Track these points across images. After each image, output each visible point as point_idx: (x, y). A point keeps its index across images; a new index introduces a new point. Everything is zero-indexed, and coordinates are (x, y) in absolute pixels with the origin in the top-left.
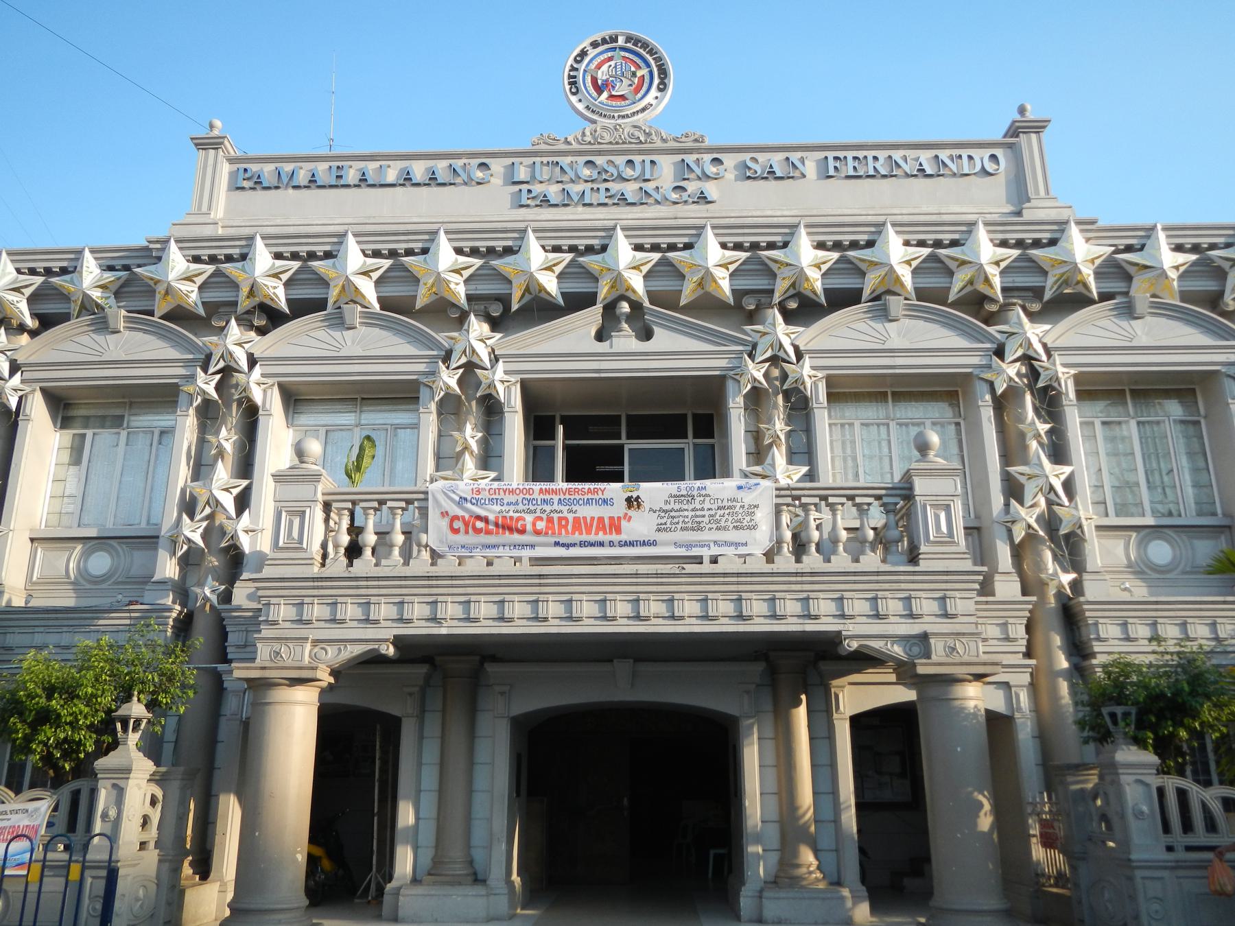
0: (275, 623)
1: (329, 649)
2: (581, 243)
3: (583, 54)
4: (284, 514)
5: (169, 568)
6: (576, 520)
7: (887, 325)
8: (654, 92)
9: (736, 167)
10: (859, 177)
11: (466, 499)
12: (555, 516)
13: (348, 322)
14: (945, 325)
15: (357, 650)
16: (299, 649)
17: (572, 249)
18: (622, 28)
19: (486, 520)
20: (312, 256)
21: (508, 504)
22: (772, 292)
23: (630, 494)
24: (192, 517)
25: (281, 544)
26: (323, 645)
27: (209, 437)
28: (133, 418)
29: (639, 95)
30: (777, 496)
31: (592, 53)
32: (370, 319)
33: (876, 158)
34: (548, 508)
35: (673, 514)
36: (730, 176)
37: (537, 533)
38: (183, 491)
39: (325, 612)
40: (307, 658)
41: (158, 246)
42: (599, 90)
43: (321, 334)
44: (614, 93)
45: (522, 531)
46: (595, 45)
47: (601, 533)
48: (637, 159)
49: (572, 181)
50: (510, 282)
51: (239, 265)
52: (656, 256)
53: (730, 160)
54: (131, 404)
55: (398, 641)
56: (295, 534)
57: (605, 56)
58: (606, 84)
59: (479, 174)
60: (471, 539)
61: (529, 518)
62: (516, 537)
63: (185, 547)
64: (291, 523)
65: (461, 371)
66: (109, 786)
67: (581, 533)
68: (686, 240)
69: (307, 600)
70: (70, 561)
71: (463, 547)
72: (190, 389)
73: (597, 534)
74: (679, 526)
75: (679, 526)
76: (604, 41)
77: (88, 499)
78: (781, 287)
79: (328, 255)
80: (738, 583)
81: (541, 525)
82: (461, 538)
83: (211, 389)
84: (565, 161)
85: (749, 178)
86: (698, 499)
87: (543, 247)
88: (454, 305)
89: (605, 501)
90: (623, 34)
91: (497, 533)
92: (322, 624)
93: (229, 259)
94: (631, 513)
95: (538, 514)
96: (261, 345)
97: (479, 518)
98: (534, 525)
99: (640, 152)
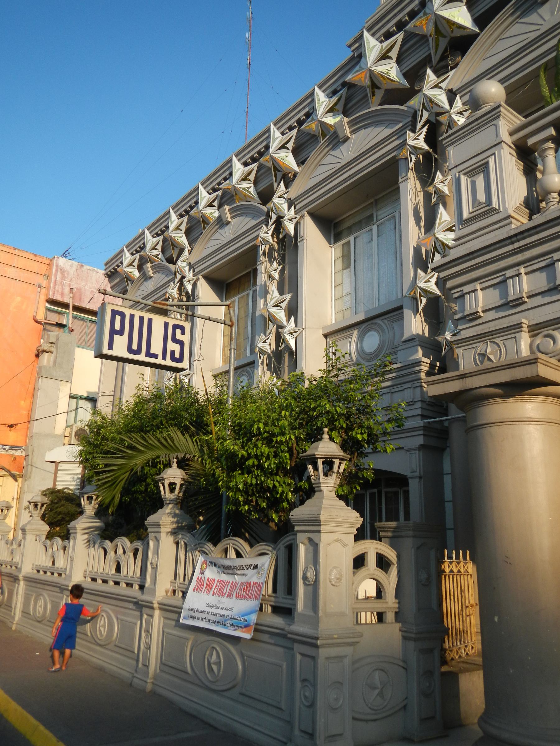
0: (474, 317)
4: (463, 178)
5: (416, 325)
16: (511, 343)
24: (425, 271)
25: (466, 215)
26: (547, 331)
27: (431, 189)
28: (379, 213)
38: (417, 250)
39: (541, 281)
40: (525, 351)
41: (357, 45)
43: (517, 28)
51: (421, 14)
54: (376, 201)
56: (481, 197)
63: (424, 300)
64: (474, 184)
66: (306, 542)
69: (509, 273)
70: (350, 346)
72: (405, 153)
77: (360, 294)
83: (422, 144)
92: (539, 300)
93: (413, 15)
96: (455, 78)
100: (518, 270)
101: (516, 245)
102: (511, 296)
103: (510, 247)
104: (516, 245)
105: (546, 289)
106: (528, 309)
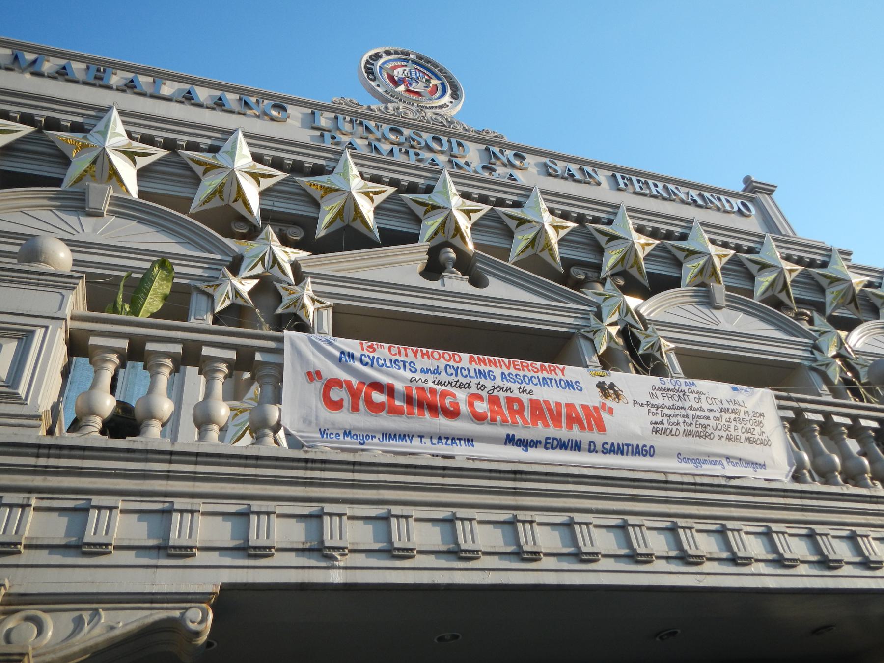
1: (48, 620)
2: (405, 179)
3: (377, 56)
6: (535, 405)
7: (715, 312)
8: (447, 99)
9: (537, 165)
10: (645, 195)
11: (351, 356)
12: (502, 395)
13: (92, 203)
14: (763, 319)
15: (126, 621)
17: (393, 183)
18: (415, 48)
19: (390, 391)
20: (53, 124)
21: (422, 371)
22: (598, 267)
23: (601, 379)
29: (435, 97)
30: (780, 407)
31: (385, 58)
32: (124, 207)
33: (656, 186)
34: (489, 384)
35: (666, 411)
36: (533, 170)
37: (479, 418)
42: (396, 84)
44: (411, 88)
45: (453, 414)
46: (388, 53)
47: (576, 427)
48: (445, 139)
49: (379, 140)
50: (317, 205)
52: (486, 208)
53: (530, 159)
55: (229, 601)
57: (399, 63)
58: (402, 81)
59: (274, 113)
60: (363, 420)
61: (461, 396)
62: (442, 423)
65: (256, 281)
67: (546, 425)
68: (515, 198)
71: (347, 433)
73: (570, 427)
74: (682, 428)
75: (682, 428)
76: (396, 53)
78: (611, 259)
79: (76, 128)
80: (803, 509)
81: (482, 407)
82: (344, 418)
84: (372, 124)
85: (550, 175)
86: (692, 396)
87: (361, 174)
88: (242, 219)
89: (569, 385)
90: (414, 53)
91: (410, 413)
94: (609, 403)
95: (474, 390)
97: (377, 386)
98: (471, 405)
99: (445, 133)
100: (29, 499)
101: (42, 461)
102: (90, 536)
103: (31, 461)
104: (42, 461)
105: (63, 542)
106: (18, 566)
